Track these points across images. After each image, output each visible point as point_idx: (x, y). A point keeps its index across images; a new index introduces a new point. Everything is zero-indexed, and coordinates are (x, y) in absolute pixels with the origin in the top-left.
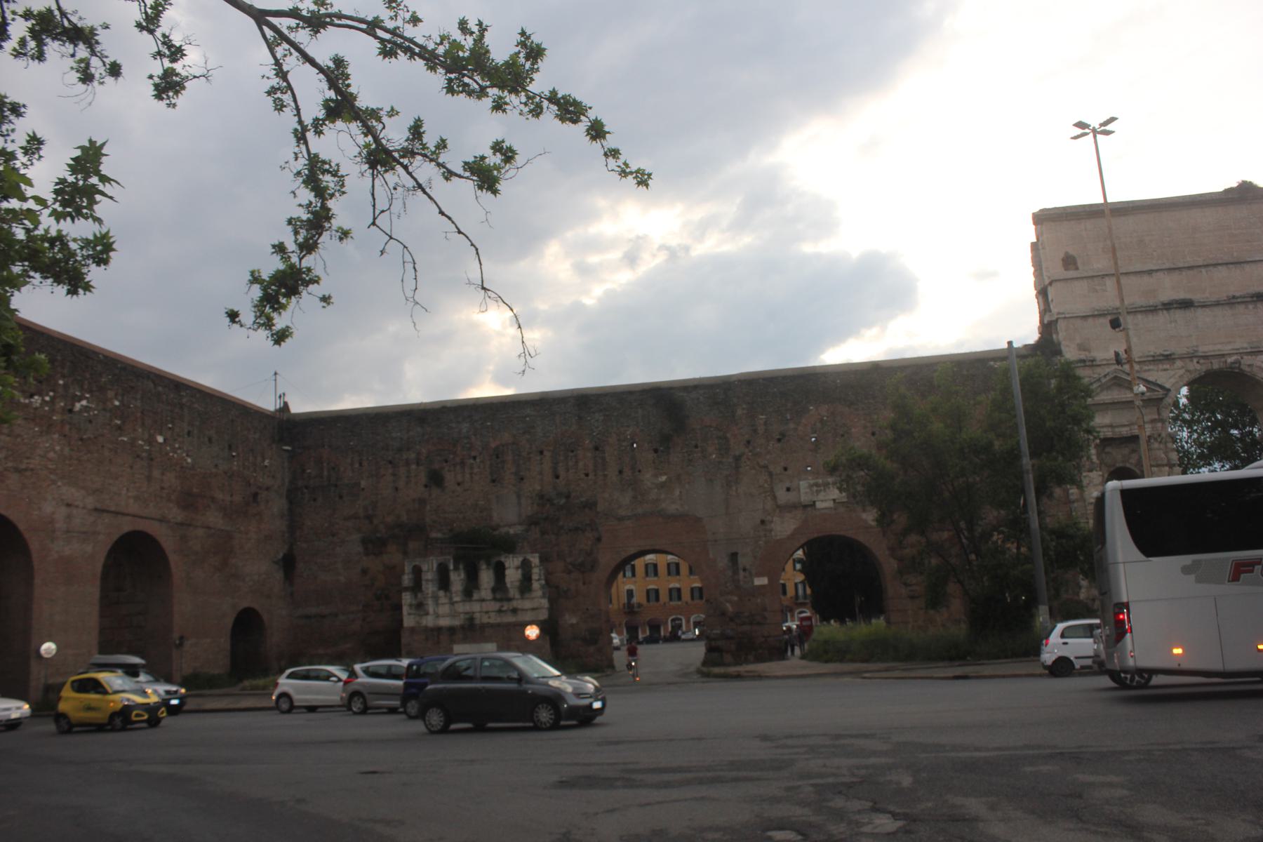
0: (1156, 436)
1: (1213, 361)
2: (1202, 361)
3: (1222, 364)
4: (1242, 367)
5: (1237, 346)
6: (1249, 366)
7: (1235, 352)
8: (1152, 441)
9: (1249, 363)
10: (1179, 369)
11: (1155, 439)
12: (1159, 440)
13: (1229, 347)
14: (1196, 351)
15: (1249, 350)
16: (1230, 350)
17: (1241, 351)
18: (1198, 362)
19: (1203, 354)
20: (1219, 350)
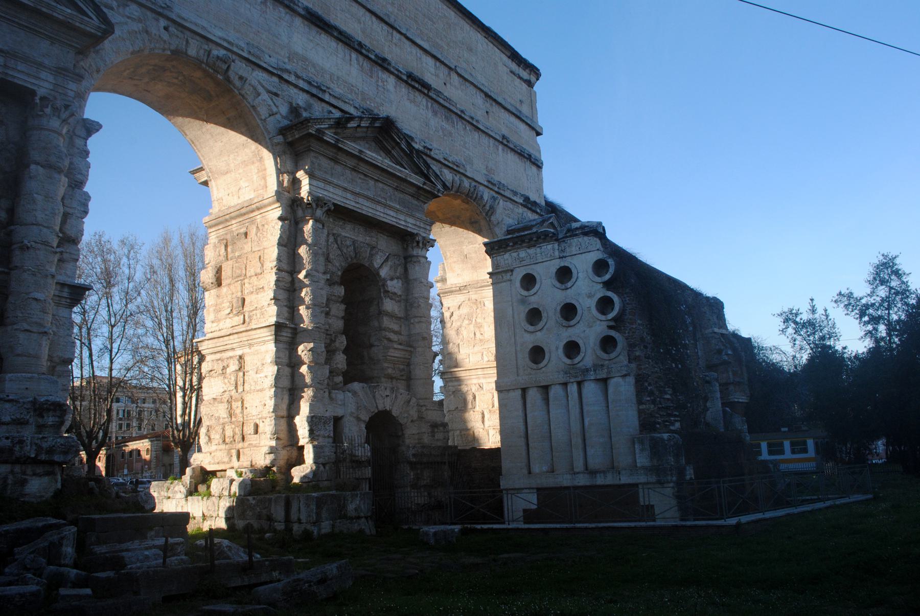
0: (59, 103)
1: (190, 40)
2: (172, 29)
3: (202, 52)
4: (231, 74)
5: (232, 36)
6: (241, 78)
7: (225, 44)
8: (48, 110)
9: (241, 73)
10: (133, 20)
11: (56, 110)
12: (64, 116)
13: (219, 33)
14: (168, 8)
15: (245, 55)
16: (220, 38)
17: (235, 49)
18: (166, 28)
19: (178, 20)
20: (203, 28)
